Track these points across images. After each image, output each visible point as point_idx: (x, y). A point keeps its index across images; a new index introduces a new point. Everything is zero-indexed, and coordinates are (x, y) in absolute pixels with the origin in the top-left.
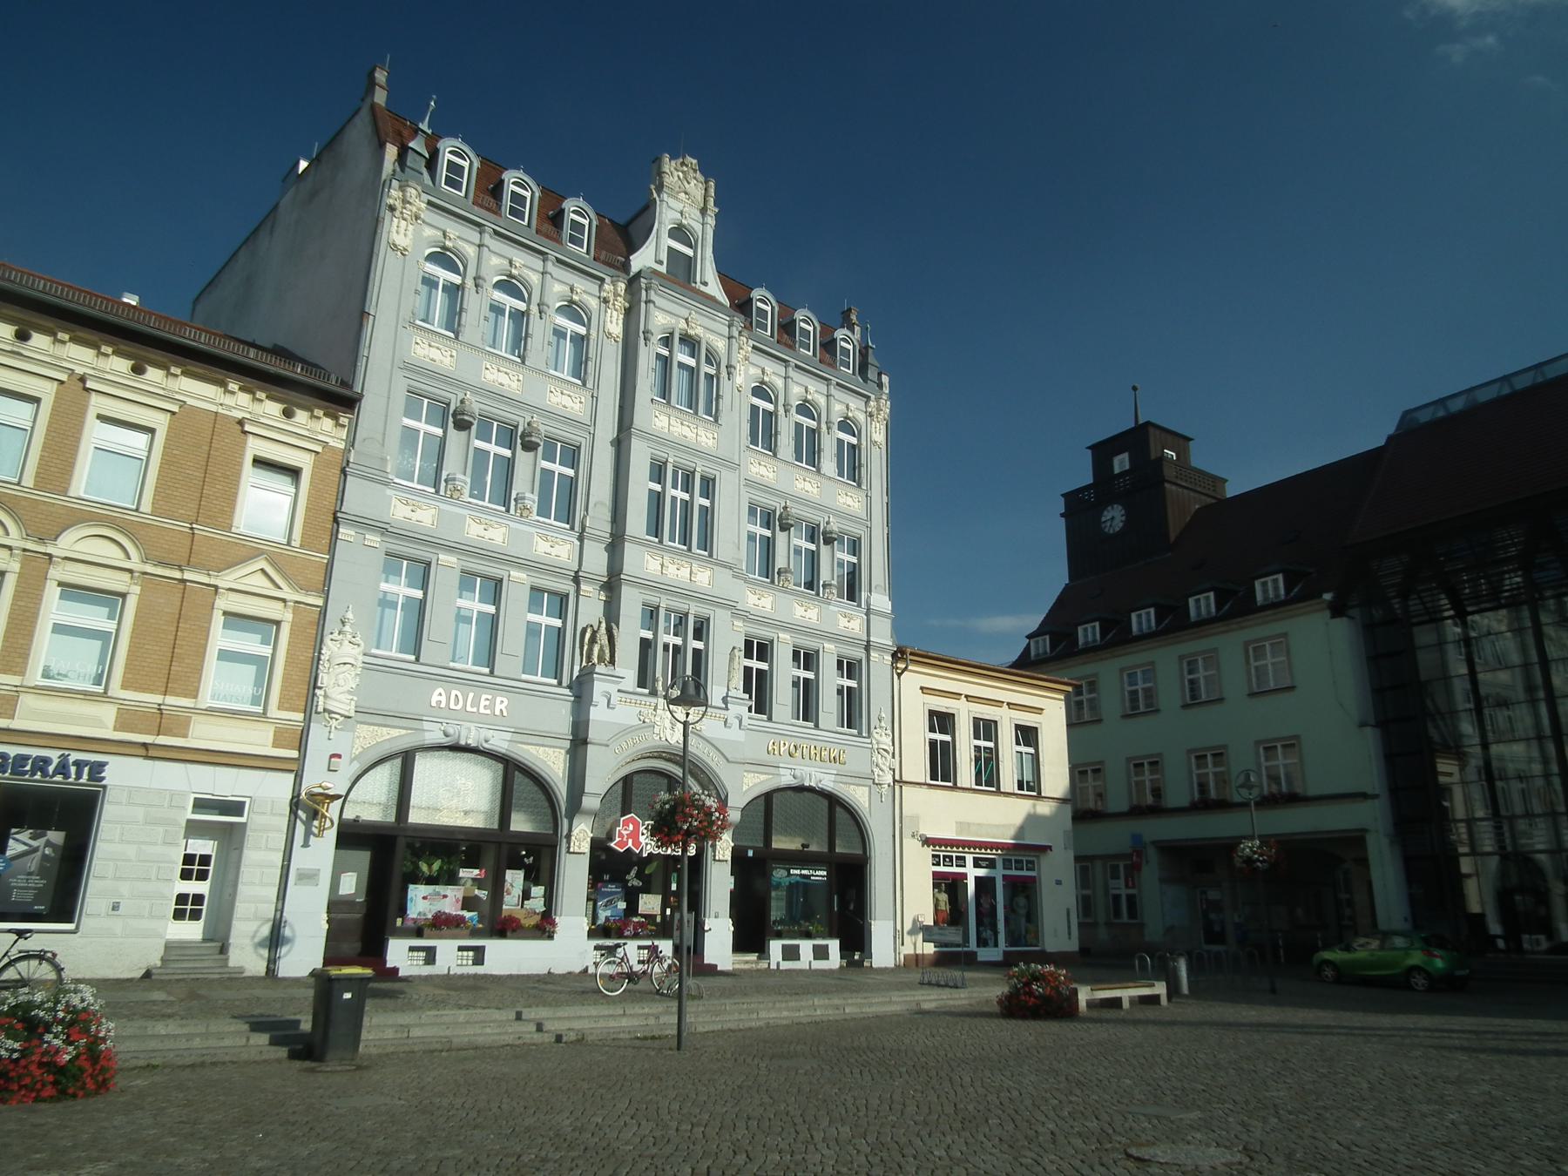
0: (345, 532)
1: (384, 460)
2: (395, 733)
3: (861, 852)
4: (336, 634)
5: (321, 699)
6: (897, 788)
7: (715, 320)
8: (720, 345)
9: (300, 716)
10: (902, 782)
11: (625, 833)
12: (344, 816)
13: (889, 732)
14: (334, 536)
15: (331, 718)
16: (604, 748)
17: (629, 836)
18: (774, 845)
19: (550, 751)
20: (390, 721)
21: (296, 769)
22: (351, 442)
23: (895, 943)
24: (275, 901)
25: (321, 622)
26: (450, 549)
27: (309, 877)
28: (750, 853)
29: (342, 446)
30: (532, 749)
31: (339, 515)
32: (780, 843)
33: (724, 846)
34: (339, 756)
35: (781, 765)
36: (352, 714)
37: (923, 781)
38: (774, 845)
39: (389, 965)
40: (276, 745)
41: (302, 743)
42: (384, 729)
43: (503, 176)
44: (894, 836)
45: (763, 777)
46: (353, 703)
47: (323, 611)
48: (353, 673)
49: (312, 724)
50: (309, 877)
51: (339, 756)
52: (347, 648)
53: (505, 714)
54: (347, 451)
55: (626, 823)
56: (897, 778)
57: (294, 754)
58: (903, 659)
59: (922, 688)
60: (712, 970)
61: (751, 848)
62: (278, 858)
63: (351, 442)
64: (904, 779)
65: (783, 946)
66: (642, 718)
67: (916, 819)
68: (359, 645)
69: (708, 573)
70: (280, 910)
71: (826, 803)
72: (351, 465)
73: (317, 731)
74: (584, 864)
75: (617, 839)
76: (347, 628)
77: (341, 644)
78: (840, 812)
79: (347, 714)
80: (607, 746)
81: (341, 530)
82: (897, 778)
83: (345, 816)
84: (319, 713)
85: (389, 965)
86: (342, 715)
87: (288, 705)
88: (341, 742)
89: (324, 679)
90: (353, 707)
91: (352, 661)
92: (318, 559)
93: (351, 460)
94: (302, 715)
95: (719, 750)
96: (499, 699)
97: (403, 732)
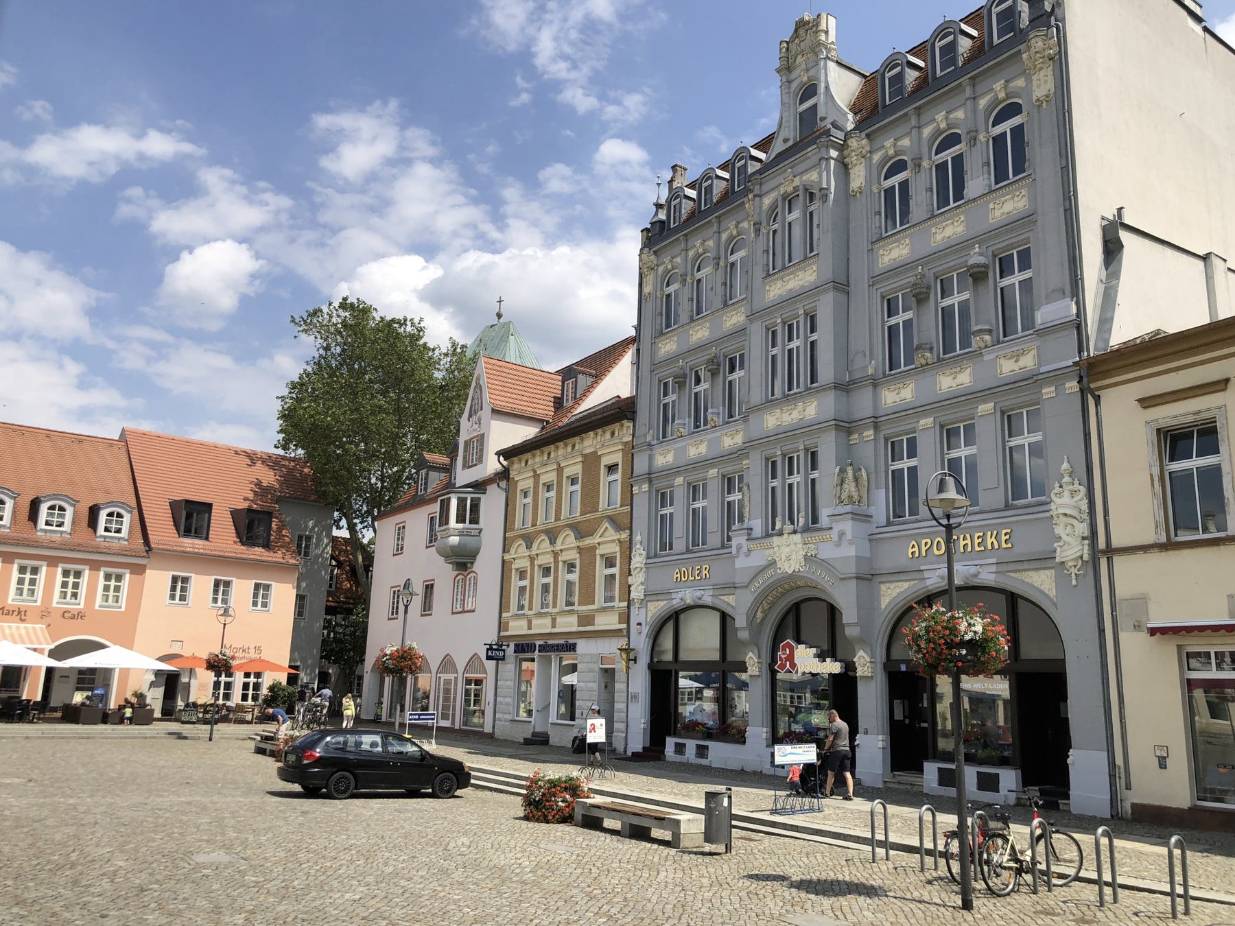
10: (1111, 552)
11: (783, 656)
14: (632, 491)
17: (787, 659)
29: (631, 439)
30: (725, 598)
33: (865, 664)
35: (922, 568)
44: (1102, 631)
45: (906, 585)
50: (635, 697)
55: (784, 649)
56: (1102, 544)
59: (1139, 400)
64: (1116, 542)
65: (940, 769)
67: (1141, 601)
75: (779, 663)
78: (1022, 607)
80: (746, 587)
82: (1102, 544)
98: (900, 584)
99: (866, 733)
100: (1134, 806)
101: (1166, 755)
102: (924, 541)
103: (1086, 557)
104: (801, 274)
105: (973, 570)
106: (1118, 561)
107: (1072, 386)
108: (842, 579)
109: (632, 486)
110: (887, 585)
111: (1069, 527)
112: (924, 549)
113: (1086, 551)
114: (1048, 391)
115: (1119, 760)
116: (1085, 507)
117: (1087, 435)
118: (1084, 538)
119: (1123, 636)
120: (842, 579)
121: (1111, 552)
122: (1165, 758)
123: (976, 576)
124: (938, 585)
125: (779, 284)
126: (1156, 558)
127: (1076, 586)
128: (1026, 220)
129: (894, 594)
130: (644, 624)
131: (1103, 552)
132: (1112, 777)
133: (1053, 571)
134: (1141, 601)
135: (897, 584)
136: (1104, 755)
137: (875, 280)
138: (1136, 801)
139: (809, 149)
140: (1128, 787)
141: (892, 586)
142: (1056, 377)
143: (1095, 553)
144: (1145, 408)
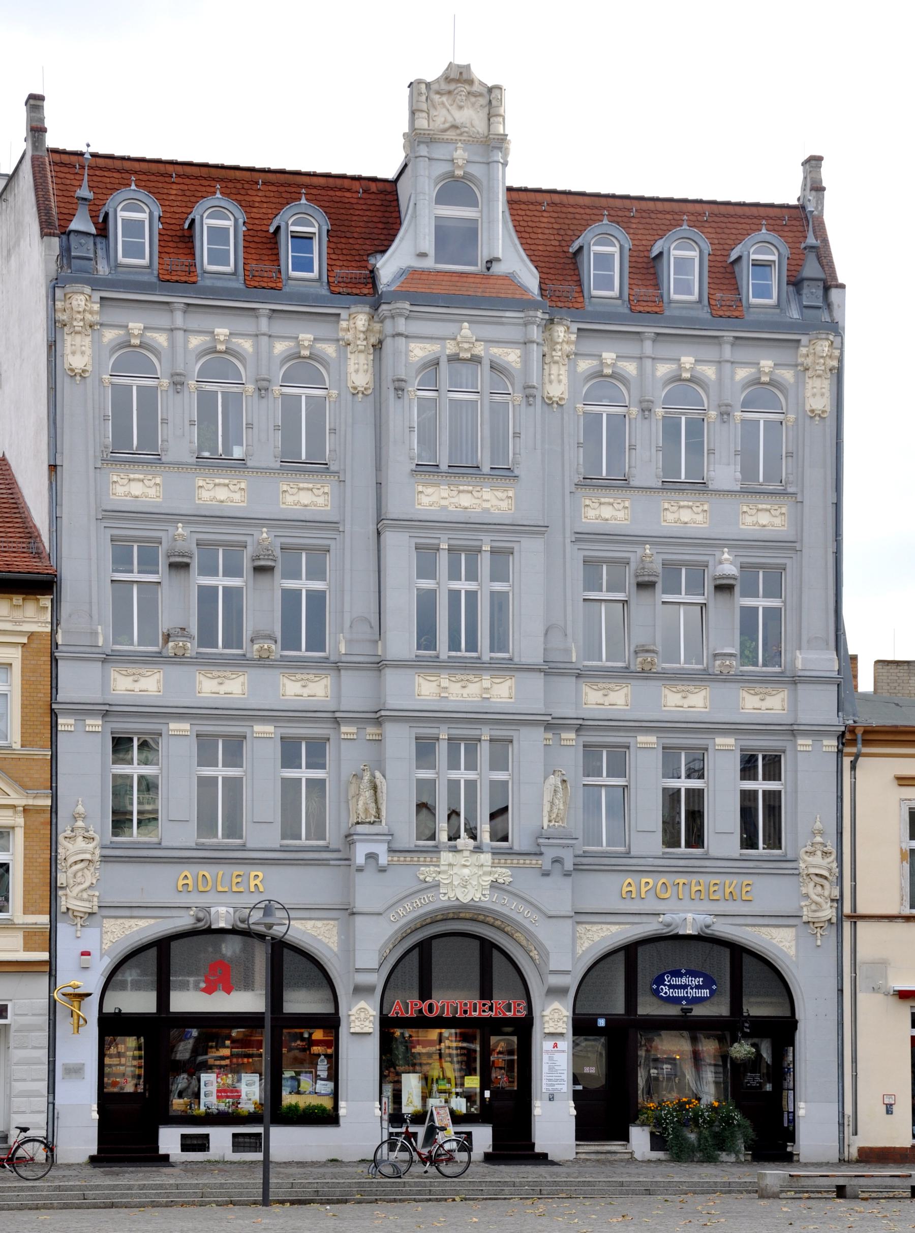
0: (64, 722)
1: (95, 634)
2: (143, 923)
3: (788, 1014)
4: (69, 832)
5: (63, 898)
6: (847, 926)
7: (502, 324)
8: (511, 357)
9: (45, 919)
10: (855, 918)
12: (105, 1011)
13: (831, 847)
14: (54, 726)
15: (76, 916)
16: (375, 918)
18: (641, 1011)
19: (319, 924)
20: (136, 912)
21: (50, 968)
22: (55, 622)
23: (841, 1131)
24: (46, 1095)
25: (54, 821)
26: (180, 716)
27: (75, 1071)
28: (602, 1023)
29: (48, 629)
31: (54, 706)
32: (647, 1008)
34: (88, 954)
36: (96, 909)
37: (894, 911)
38: (641, 1011)
39: (162, 1151)
40: (27, 948)
41: (52, 946)
42: (133, 920)
43: (196, 214)
44: (841, 991)
45: (614, 929)
46: (96, 899)
47: (54, 809)
48: (92, 869)
49: (58, 924)
50: (75, 1071)
51: (88, 954)
52: (80, 843)
53: (261, 889)
54: (53, 633)
56: (847, 910)
57: (45, 956)
58: (853, 742)
60: (543, 1159)
61: (601, 1016)
62: (43, 1054)
63: (55, 622)
64: (861, 910)
66: (422, 877)
67: (882, 964)
68: (93, 838)
69: (509, 683)
70: (52, 1104)
71: (726, 953)
72: (60, 648)
73: (64, 931)
74: (372, 1047)
76: (80, 823)
77: (75, 840)
79: (90, 911)
80: (380, 914)
81: (60, 721)
82: (847, 910)
83: (105, 1011)
84: (64, 913)
85: (162, 1151)
86: (85, 913)
87: (33, 909)
88: (90, 938)
89: (61, 879)
90: (96, 903)
91: (88, 856)
92: (40, 757)
93: (60, 642)
94: (48, 916)
95: (531, 904)
96: (253, 874)
97: (152, 921)
98: (605, 927)
99: (551, 1098)
100: (861, 1150)
101: (893, 1102)
102: (644, 881)
103: (834, 920)
104: (487, 494)
105: (709, 920)
106: (863, 927)
107: (831, 744)
108: (550, 917)
109: (54, 714)
110: (589, 927)
111: (819, 888)
112: (643, 890)
113: (835, 914)
114: (804, 743)
115: (848, 1110)
116: (836, 871)
117: (840, 798)
118: (832, 900)
119: (860, 996)
120: (550, 917)
121: (855, 918)
122: (891, 1105)
123: (708, 927)
124: (659, 932)
125: (444, 491)
126: (900, 928)
127: (819, 946)
128: (790, 546)
129: (596, 938)
130: (95, 953)
131: (849, 917)
132: (841, 1125)
133: (794, 930)
134: (882, 964)
135: (599, 926)
136: (835, 1107)
137: (581, 537)
138: (862, 1145)
139: (508, 314)
140: (855, 1133)
141: (595, 928)
142: (817, 732)
143: (841, 917)
144: (900, 785)
